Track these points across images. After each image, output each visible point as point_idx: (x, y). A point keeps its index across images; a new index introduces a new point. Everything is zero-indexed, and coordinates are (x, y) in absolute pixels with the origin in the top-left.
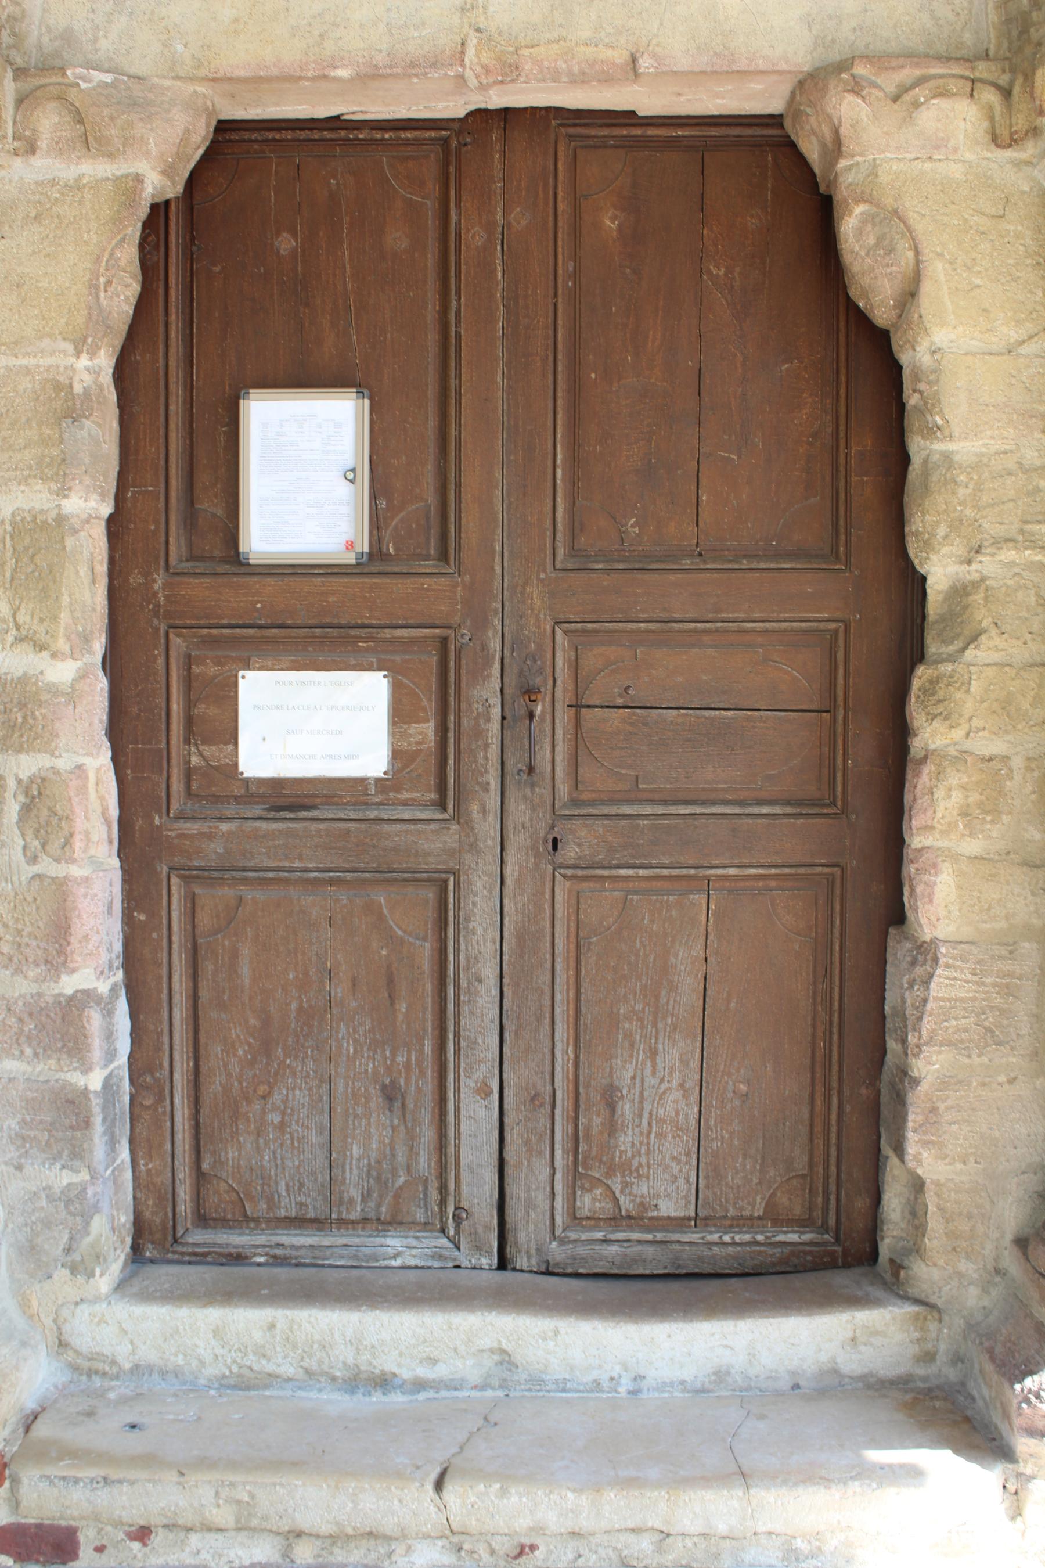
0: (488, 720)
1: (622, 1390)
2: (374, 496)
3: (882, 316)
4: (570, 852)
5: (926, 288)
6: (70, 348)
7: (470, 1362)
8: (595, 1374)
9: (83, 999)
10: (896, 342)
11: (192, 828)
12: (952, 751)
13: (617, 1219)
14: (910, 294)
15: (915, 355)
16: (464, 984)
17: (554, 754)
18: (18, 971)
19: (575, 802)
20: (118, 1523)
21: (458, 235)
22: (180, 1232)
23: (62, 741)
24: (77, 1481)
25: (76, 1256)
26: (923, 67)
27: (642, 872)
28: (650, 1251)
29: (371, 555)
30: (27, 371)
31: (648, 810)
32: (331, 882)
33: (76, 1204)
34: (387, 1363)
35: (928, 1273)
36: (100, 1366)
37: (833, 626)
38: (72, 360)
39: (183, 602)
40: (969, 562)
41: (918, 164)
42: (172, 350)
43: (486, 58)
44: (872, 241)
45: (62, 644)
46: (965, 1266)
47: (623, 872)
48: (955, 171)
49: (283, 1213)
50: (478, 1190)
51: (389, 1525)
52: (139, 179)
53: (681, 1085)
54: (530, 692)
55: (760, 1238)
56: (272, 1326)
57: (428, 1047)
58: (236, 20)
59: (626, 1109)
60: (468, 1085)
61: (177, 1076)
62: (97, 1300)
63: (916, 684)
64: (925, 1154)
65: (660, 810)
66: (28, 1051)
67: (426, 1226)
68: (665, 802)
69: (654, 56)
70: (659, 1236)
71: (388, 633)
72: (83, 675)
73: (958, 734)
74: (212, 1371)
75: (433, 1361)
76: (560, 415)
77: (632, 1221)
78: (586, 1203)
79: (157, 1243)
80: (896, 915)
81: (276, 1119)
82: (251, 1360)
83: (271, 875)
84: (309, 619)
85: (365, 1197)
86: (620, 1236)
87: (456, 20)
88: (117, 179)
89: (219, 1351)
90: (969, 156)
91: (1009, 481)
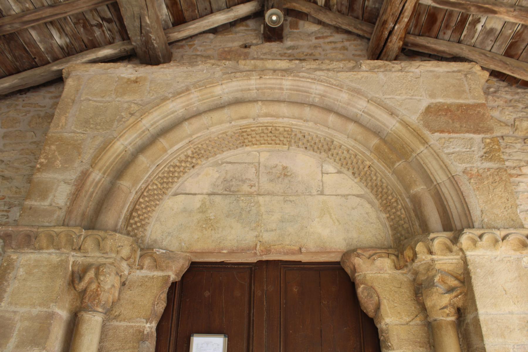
3: (371, 314)
5: (382, 307)
6: (145, 321)
10: (376, 321)
14: (378, 308)
15: (382, 325)
26: (375, 250)
38: (145, 324)
43: (262, 248)
44: (366, 294)
48: (387, 276)
52: (169, 276)
58: (198, 238)
69: (306, 248)
76: (282, 343)
87: (255, 239)
88: (163, 277)
90: (390, 272)
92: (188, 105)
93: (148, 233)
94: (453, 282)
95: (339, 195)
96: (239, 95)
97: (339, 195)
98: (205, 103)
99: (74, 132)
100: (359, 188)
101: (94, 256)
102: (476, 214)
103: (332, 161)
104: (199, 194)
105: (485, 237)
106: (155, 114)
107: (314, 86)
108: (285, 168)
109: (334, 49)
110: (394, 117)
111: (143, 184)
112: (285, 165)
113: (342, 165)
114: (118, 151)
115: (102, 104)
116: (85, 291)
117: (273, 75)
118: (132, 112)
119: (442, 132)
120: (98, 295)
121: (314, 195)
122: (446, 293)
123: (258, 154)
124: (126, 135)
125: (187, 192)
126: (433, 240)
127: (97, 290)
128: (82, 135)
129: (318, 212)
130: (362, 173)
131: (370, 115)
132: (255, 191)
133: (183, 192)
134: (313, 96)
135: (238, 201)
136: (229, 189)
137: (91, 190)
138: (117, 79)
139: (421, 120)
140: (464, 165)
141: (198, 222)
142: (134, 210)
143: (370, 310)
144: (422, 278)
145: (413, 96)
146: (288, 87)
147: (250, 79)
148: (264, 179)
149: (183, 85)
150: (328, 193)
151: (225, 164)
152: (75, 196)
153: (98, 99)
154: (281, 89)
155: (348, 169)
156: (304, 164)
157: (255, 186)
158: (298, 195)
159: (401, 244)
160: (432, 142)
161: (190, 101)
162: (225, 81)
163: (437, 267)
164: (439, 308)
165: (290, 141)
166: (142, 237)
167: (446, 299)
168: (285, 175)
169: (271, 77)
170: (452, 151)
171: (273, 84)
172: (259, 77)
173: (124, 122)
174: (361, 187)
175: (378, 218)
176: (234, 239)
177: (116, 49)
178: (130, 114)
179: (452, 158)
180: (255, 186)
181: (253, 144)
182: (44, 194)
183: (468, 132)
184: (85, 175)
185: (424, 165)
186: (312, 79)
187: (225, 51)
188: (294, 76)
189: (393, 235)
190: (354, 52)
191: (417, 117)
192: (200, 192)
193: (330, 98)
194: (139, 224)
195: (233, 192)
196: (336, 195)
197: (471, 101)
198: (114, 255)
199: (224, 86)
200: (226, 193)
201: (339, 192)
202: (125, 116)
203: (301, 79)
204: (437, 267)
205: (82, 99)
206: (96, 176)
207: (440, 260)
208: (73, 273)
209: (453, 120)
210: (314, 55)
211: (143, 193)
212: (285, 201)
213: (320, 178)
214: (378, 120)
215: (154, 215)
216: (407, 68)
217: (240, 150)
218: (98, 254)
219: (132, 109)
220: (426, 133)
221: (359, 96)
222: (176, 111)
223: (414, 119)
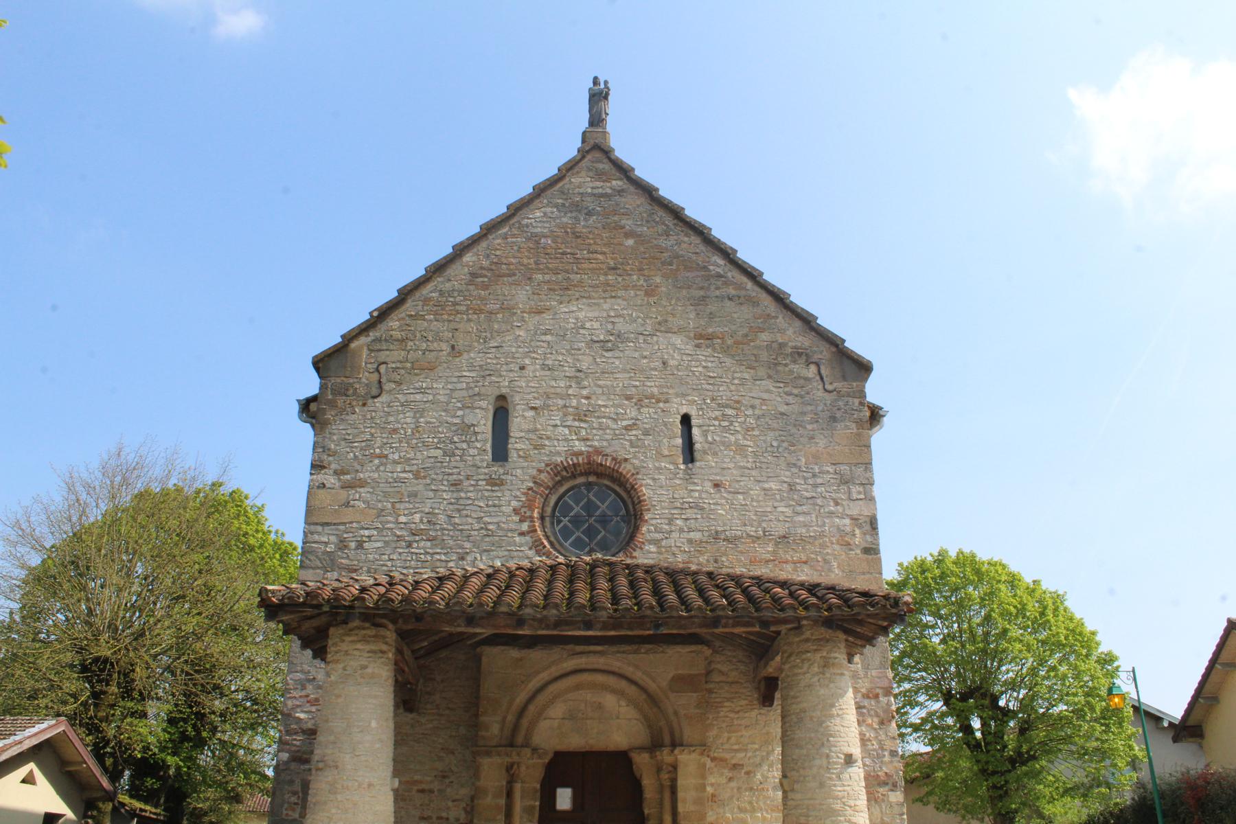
26: (642, 749)
101: (515, 758)
102: (685, 737)
129: (616, 725)
136: (571, 716)
143: (638, 775)
152: (502, 730)
156: (610, 701)
159: (654, 745)
176: (575, 742)
184: (504, 718)
223: (664, 684)
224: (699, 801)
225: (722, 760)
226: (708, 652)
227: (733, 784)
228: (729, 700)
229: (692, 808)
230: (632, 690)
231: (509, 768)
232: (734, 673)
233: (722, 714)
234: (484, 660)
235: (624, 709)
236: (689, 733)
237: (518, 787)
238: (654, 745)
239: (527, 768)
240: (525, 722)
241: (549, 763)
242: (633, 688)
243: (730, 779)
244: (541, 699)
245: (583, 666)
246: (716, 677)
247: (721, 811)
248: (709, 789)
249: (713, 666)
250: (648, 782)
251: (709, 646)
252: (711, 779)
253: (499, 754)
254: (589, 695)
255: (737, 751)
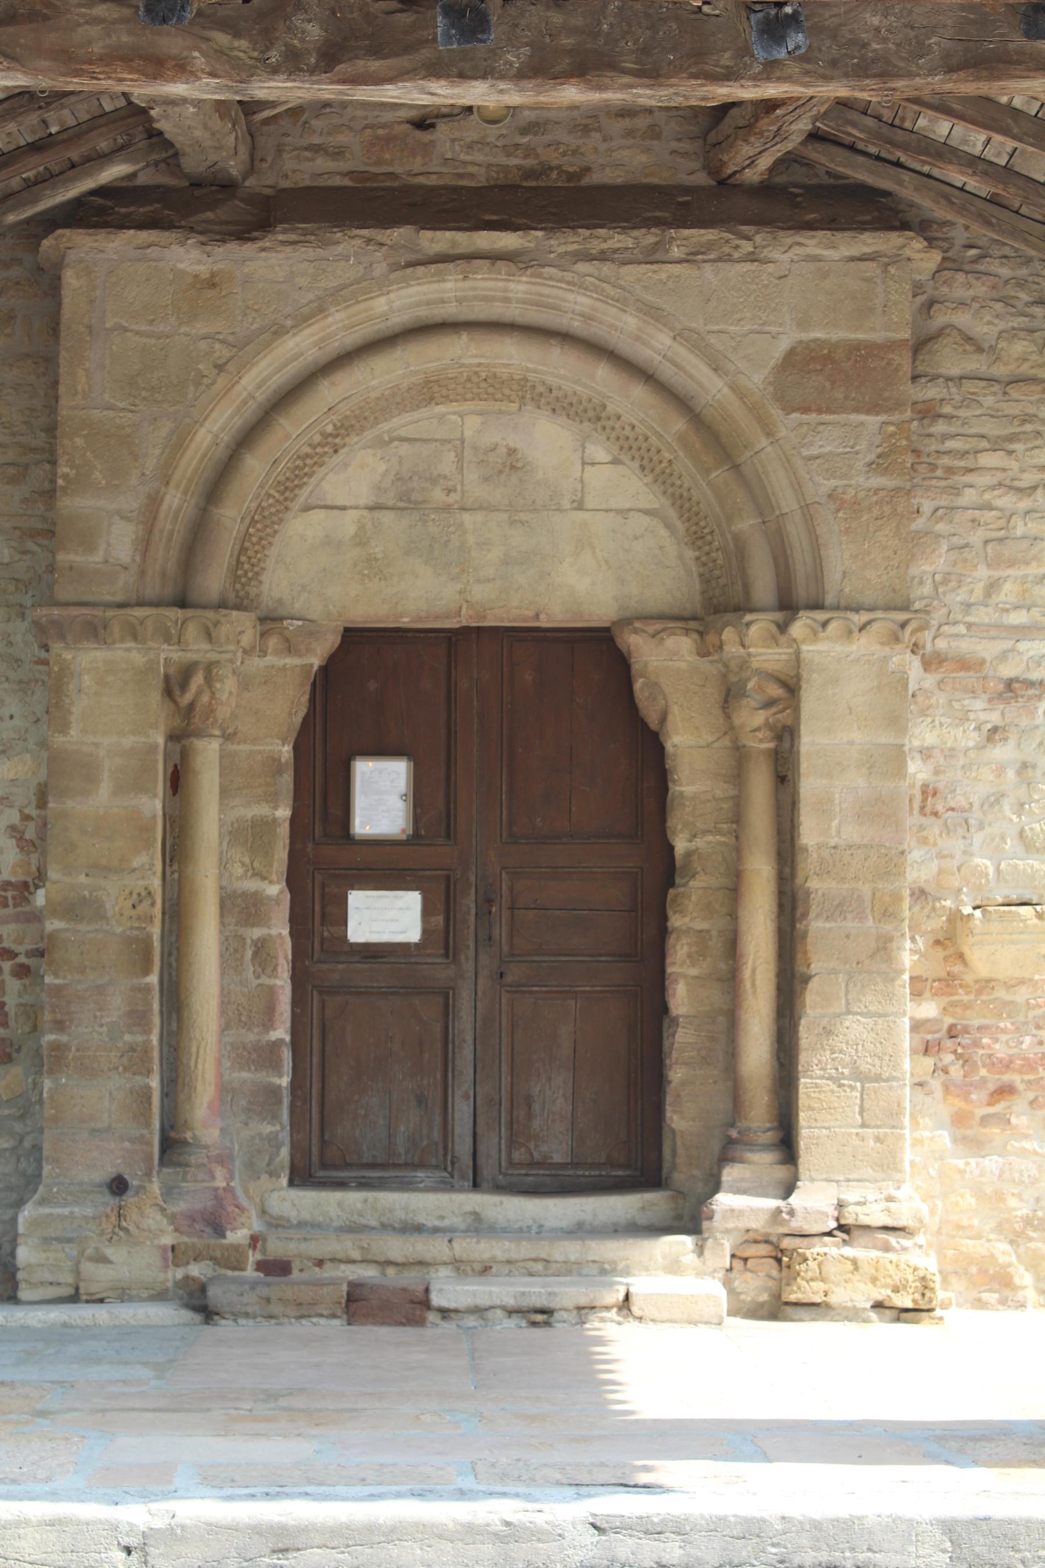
0: (469, 915)
1: (533, 1232)
2: (415, 807)
4: (509, 979)
5: (670, 717)
6: (280, 742)
7: (460, 1219)
8: (520, 1224)
9: (281, 1041)
10: (662, 738)
11: (325, 967)
12: (684, 928)
13: (533, 1164)
15: (669, 747)
16: (457, 1043)
17: (501, 931)
18: (249, 1029)
19: (512, 955)
20: (309, 1258)
21: (456, 684)
22: (313, 1171)
23: (273, 922)
24: (292, 1239)
25: (272, 1168)
27: (544, 989)
28: (548, 1179)
29: (413, 835)
30: (260, 752)
31: (546, 958)
32: (392, 994)
33: (273, 1141)
34: (421, 1219)
35: (679, 1177)
36: (281, 1223)
37: (635, 870)
38: (280, 748)
39: (325, 857)
40: (691, 841)
41: (666, 663)
42: (317, 736)
43: (470, 612)
44: (647, 694)
45: (274, 877)
46: (696, 1172)
47: (534, 989)
48: (683, 665)
49: (365, 1161)
50: (463, 1147)
51: (428, 1257)
52: (312, 665)
53: (564, 1095)
54: (489, 901)
55: (603, 1173)
56: (366, 1201)
57: (439, 1075)
58: (357, 596)
59: (536, 1107)
60: (458, 1094)
61: (314, 1091)
62: (282, 1189)
63: (669, 897)
64: (675, 1117)
65: (552, 958)
66: (253, 1068)
67: (437, 1167)
68: (555, 955)
69: (547, 614)
70: (553, 1172)
71: (421, 873)
72: (281, 892)
73: (687, 920)
74: (336, 1224)
75: (442, 1218)
76: (504, 770)
77: (539, 1164)
78: (518, 1155)
79: (302, 1176)
80: (665, 1009)
81: (362, 1112)
82: (355, 1218)
83: (363, 990)
84: (385, 866)
85: (407, 1153)
86: (534, 1172)
87: (457, 597)
88: (303, 666)
89: (340, 1213)
90: (689, 658)
91: (708, 804)
92: (323, 340)
93: (265, 588)
94: (775, 691)
95: (611, 510)
96: (426, 314)
97: (611, 510)
98: (355, 332)
99: (112, 408)
100: (651, 496)
101: (198, 650)
103: (603, 438)
104: (351, 508)
105: (832, 626)
106: (263, 364)
107: (571, 297)
108: (512, 452)
109: (629, 133)
110: (720, 376)
111: (251, 501)
112: (512, 445)
113: (621, 449)
114: (204, 447)
115: (153, 341)
116: (191, 706)
117: (490, 273)
118: (219, 362)
119: (806, 410)
120: (212, 711)
121: (566, 510)
122: (761, 708)
123: (459, 419)
124: (214, 414)
125: (329, 503)
126: (748, 625)
127: (210, 703)
128: (130, 415)
130: (658, 470)
131: (676, 365)
132: (457, 502)
133: (320, 503)
134: (570, 315)
135: (426, 521)
136: (404, 498)
137: (169, 527)
138: (171, 277)
139: (770, 383)
140: (833, 483)
141: (355, 565)
142: (243, 550)
144: (734, 679)
145: (764, 324)
146: (519, 295)
147: (444, 281)
148: (472, 475)
149: (311, 296)
150: (590, 507)
151: (396, 443)
152: (145, 545)
153: (143, 328)
154: (507, 300)
155: (633, 458)
156: (548, 443)
157: (455, 491)
158: (536, 510)
159: (715, 608)
160: (783, 432)
161: (328, 331)
162: (395, 287)
163: (755, 665)
164: (749, 729)
165: (523, 397)
166: (257, 595)
167: (760, 718)
168: (513, 467)
169: (486, 276)
170: (816, 452)
171: (490, 289)
172: (461, 277)
173: (208, 386)
174: (654, 494)
175: (680, 557)
176: (419, 594)
177: (138, 163)
178: (216, 366)
179: (814, 467)
180: (455, 491)
181: (451, 401)
182: (88, 541)
183: (857, 410)
184: (154, 501)
185: (763, 477)
186: (568, 283)
187: (378, 138)
188: (531, 276)
189: (703, 593)
190: (674, 145)
191: (762, 377)
192: (353, 503)
193: (601, 323)
194: (250, 575)
195: (416, 502)
196: (607, 511)
197: (878, 336)
198: (232, 647)
199: (392, 296)
200: (402, 504)
201: (613, 504)
202: (206, 372)
203: (547, 282)
204: (755, 665)
205: (108, 325)
206: (173, 499)
207: (761, 654)
208: (167, 678)
209: (833, 383)
210: (582, 154)
211: (253, 517)
212: (512, 523)
213: (578, 475)
214: (691, 376)
215: (273, 552)
216: (765, 250)
217: (423, 413)
218: (205, 646)
219: (217, 355)
220: (776, 412)
221: (657, 324)
222: (302, 354)
223: (757, 379)
224: (879, 810)
225: (965, 664)
226: (923, 259)
227: (1003, 752)
228: (997, 444)
229: (852, 833)
230: (631, 402)
231: (174, 685)
232: (1019, 347)
233: (969, 496)
234: (71, 279)
235: (600, 477)
236: (847, 562)
237: (208, 754)
238: (715, 608)
239: (245, 685)
240: (232, 515)
241: (325, 670)
242: (639, 391)
243: (994, 734)
244: (294, 429)
245: (450, 311)
246: (951, 361)
247: (955, 845)
248: (917, 770)
249: (940, 319)
250: (690, 744)
251: (931, 242)
252: (923, 734)
253: (133, 633)
254: (472, 423)
255: (1022, 632)
